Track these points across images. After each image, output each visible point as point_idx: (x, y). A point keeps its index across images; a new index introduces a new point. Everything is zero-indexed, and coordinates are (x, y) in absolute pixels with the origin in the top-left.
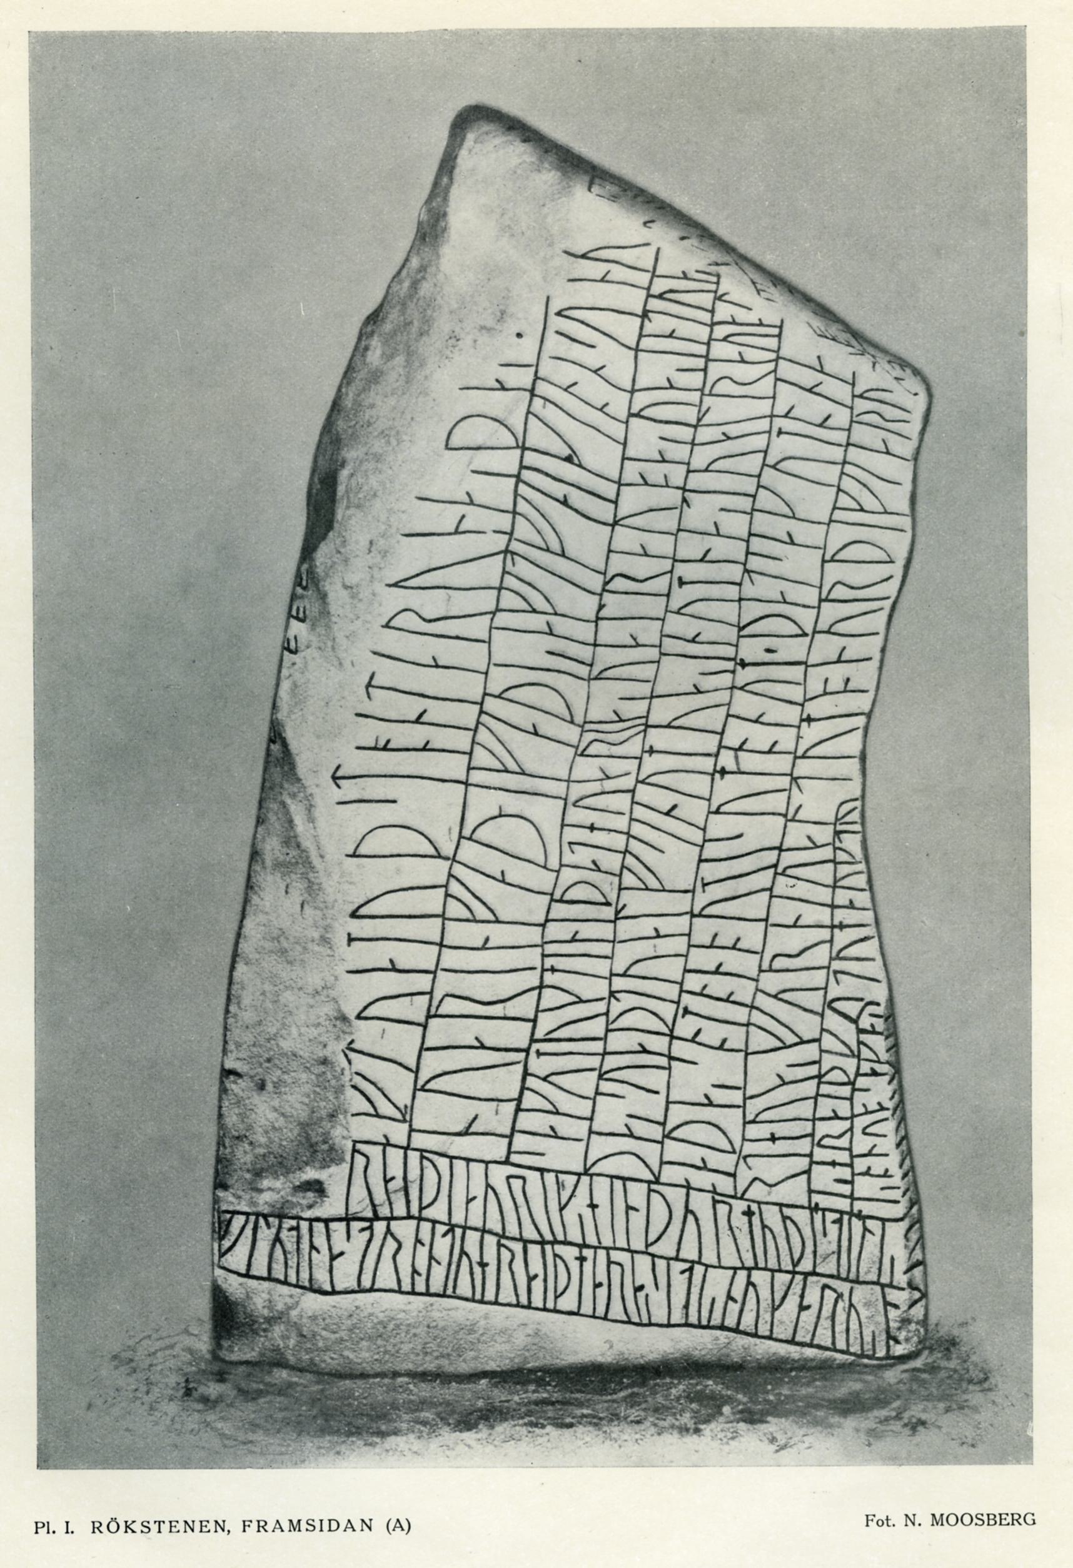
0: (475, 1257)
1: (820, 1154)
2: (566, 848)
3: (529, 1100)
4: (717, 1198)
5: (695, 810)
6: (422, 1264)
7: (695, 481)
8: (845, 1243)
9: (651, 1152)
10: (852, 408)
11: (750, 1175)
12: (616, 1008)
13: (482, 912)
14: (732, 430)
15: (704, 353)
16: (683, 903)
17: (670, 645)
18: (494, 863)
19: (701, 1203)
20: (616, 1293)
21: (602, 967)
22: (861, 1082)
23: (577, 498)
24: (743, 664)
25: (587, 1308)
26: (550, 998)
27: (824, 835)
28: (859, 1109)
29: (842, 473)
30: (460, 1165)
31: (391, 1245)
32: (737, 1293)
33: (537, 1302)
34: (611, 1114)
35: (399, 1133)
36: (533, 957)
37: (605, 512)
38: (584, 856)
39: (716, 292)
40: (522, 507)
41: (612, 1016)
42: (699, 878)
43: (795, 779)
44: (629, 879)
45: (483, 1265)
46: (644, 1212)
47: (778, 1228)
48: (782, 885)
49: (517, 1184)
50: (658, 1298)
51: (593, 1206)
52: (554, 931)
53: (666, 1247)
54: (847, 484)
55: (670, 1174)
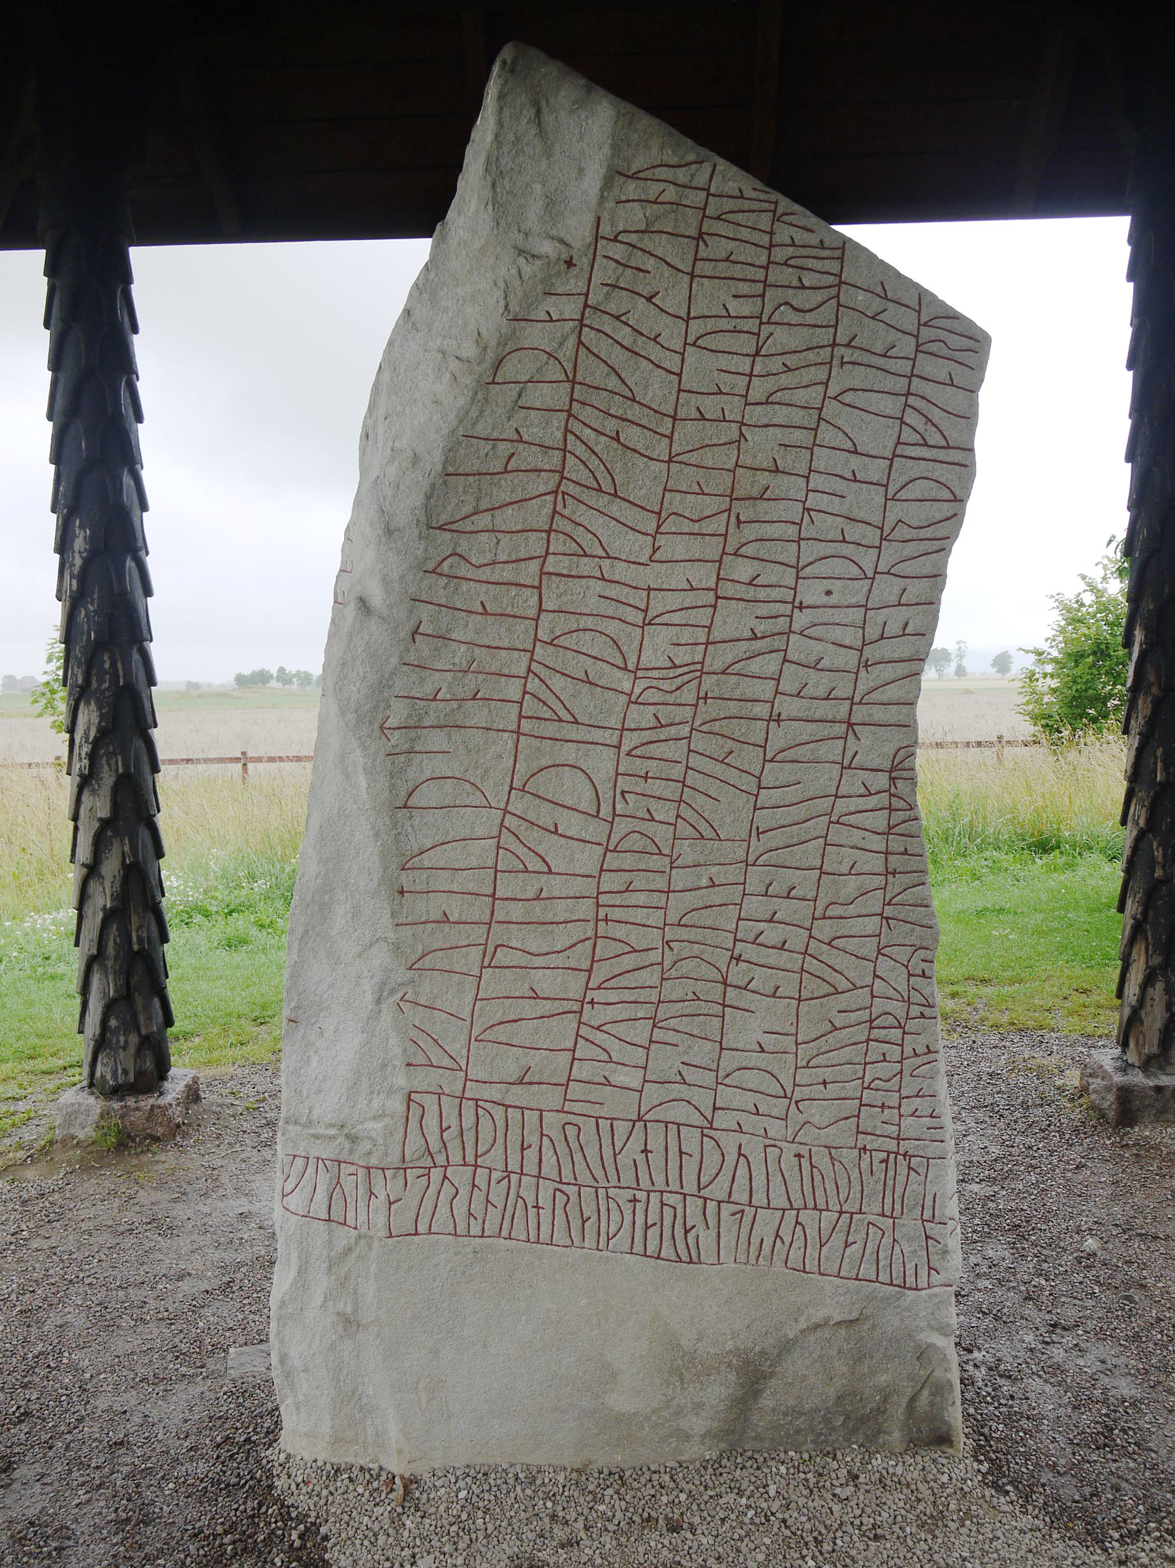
0: (530, 1202)
2: (618, 797)
3: (583, 1050)
5: (750, 758)
6: (477, 1207)
8: (890, 1183)
10: (917, 337)
11: (802, 1118)
13: (535, 864)
14: (791, 360)
15: (763, 278)
17: (727, 589)
19: (754, 1150)
20: (667, 1233)
21: (656, 918)
23: (631, 435)
24: (801, 608)
25: (638, 1247)
27: (882, 781)
28: (908, 1051)
29: (906, 405)
31: (447, 1189)
32: (785, 1233)
34: (664, 1062)
36: (585, 908)
37: (661, 449)
39: (774, 212)
41: (667, 965)
42: (754, 827)
43: (850, 725)
44: (684, 829)
45: (537, 1207)
49: (571, 1131)
50: (707, 1238)
52: (609, 882)
53: (718, 1190)
54: (911, 418)
55: (721, 1120)
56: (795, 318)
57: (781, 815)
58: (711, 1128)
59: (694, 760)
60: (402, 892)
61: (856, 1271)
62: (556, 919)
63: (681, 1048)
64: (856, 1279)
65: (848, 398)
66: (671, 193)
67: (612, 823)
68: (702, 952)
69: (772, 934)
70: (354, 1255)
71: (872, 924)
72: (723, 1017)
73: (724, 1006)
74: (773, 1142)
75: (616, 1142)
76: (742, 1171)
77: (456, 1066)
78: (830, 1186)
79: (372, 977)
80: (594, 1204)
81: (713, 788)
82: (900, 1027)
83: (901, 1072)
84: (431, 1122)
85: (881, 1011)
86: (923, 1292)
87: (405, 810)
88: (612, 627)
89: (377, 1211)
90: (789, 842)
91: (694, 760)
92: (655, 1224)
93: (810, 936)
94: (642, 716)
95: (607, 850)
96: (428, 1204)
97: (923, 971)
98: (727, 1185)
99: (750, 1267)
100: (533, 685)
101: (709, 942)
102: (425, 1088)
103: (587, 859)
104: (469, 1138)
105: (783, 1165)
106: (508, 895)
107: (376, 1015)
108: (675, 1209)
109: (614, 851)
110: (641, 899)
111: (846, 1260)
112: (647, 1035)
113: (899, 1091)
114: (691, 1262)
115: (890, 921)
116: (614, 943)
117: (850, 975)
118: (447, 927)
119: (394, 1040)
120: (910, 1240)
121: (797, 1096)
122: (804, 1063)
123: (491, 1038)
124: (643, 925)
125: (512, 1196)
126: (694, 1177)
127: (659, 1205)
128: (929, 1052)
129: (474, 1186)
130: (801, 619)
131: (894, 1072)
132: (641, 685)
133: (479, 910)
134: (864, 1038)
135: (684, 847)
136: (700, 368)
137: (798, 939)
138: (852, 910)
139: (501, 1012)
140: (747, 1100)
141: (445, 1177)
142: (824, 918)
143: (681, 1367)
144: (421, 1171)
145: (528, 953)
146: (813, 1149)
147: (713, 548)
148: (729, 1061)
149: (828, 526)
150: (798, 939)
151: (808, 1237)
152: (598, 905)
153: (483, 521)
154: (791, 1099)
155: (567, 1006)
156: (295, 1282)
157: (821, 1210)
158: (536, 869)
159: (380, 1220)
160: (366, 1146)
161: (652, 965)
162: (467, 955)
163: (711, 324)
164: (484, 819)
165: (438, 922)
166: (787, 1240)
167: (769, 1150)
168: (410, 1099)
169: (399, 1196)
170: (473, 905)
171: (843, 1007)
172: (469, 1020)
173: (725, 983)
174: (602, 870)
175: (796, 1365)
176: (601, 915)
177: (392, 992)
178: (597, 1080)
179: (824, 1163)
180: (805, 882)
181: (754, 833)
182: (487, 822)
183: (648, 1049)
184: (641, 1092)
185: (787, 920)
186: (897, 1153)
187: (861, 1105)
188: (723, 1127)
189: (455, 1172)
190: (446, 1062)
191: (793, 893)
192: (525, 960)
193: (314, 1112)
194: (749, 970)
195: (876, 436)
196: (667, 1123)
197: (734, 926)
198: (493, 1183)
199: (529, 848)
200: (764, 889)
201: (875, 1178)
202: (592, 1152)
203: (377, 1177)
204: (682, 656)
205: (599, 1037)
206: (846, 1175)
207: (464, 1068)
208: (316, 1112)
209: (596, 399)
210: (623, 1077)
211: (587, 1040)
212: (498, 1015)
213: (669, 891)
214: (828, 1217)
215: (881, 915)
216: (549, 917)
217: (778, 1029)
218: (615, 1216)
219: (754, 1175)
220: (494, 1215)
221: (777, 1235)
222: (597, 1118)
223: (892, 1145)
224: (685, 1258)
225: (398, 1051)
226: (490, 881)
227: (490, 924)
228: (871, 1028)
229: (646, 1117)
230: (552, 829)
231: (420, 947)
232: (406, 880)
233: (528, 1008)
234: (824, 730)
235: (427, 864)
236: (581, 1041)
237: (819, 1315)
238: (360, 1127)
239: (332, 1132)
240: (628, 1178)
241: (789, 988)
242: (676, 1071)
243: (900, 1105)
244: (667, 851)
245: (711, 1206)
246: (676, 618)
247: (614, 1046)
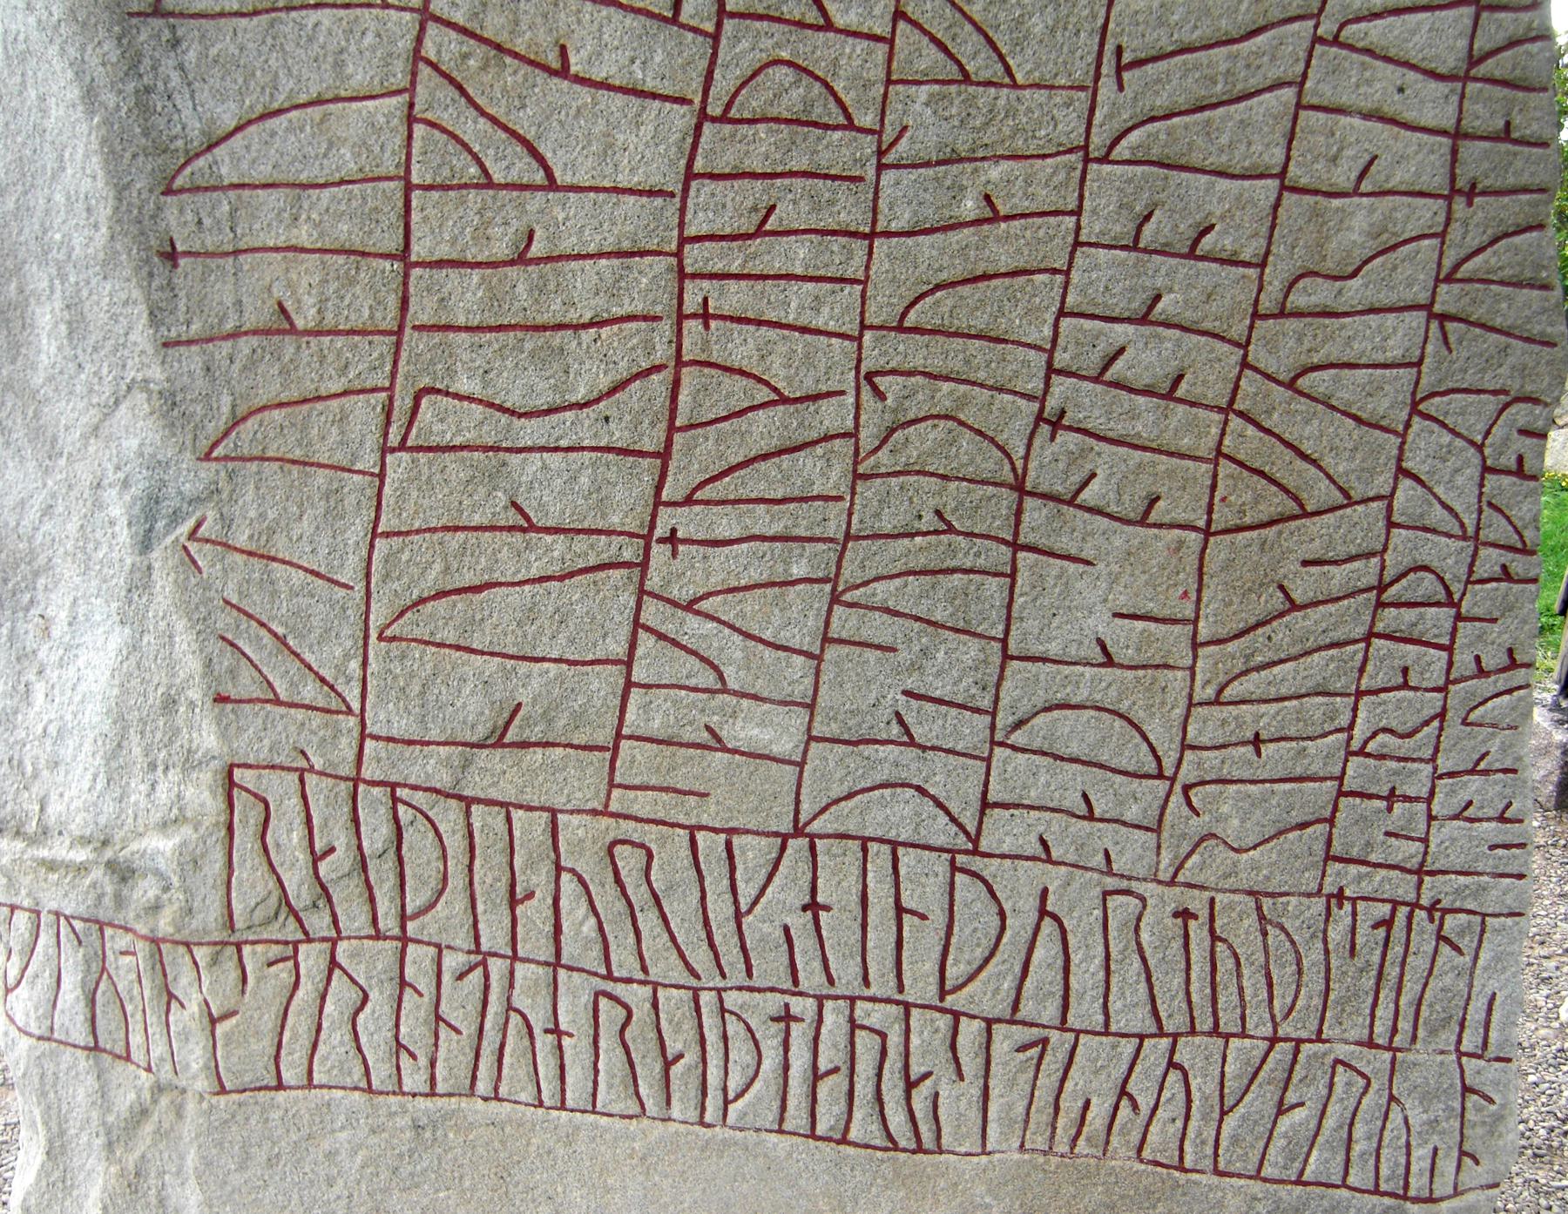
0: (539, 1021)
3: (651, 661)
4: (1117, 885)
6: (414, 1028)
8: (1392, 972)
11: (1196, 825)
13: (510, 165)
20: (864, 1089)
21: (837, 309)
22: (1476, 600)
28: (1464, 660)
34: (860, 689)
36: (647, 284)
41: (867, 438)
45: (556, 1031)
46: (938, 918)
49: (629, 860)
50: (957, 1101)
51: (813, 907)
53: (987, 995)
55: (1002, 832)
58: (975, 852)
60: (171, 256)
61: (1297, 1165)
62: (572, 316)
63: (903, 656)
64: (1299, 1182)
67: (716, 37)
68: (962, 402)
69: (1147, 357)
70: (148, 1128)
72: (1013, 575)
73: (1016, 546)
74: (1124, 884)
75: (740, 885)
76: (1046, 951)
77: (335, 704)
78: (1252, 981)
79: (126, 484)
80: (689, 1026)
82: (1450, 603)
83: (1442, 715)
84: (288, 837)
85: (1407, 562)
86: (1444, 1205)
87: (157, 23)
89: (186, 1036)
90: (1202, 93)
92: (836, 1070)
93: (1245, 364)
95: (703, 116)
96: (298, 1023)
97: (1520, 459)
98: (1008, 985)
99: (1054, 1160)
101: (981, 376)
102: (264, 756)
103: (647, 145)
105: (1145, 936)
106: (444, 252)
107: (141, 581)
108: (883, 1036)
109: (724, 119)
110: (799, 254)
111: (1278, 1143)
112: (814, 623)
113: (1433, 759)
114: (919, 1149)
115: (1450, 326)
116: (728, 380)
117: (1339, 468)
118: (289, 345)
119: (184, 641)
120: (1426, 1098)
121: (1187, 774)
122: (1210, 692)
123: (417, 633)
124: (804, 330)
126: (931, 966)
127: (846, 1027)
128: (1513, 664)
129: (403, 983)
131: (1428, 712)
133: (368, 297)
134: (1360, 631)
135: (916, 105)
137: (1210, 371)
138: (1355, 292)
139: (438, 567)
140: (1068, 784)
141: (333, 964)
142: (1282, 314)
144: (276, 951)
145: (501, 409)
146: (1219, 897)
150: (1210, 371)
151: (1196, 1095)
152: (682, 275)
154: (1173, 780)
155: (606, 549)
156: (44, 1172)
157: (1227, 1037)
158: (513, 177)
159: (195, 1056)
160: (145, 890)
161: (827, 438)
162: (343, 418)
164: (369, 39)
165: (267, 332)
166: (1145, 1103)
167: (1113, 901)
168: (230, 784)
169: (230, 1005)
170: (352, 282)
171: (1314, 550)
172: (360, 587)
173: (1019, 487)
174: (690, 176)
176: (692, 303)
177: (176, 518)
178: (688, 735)
179: (1241, 928)
181: (1107, 68)
183: (819, 658)
184: (801, 765)
185: (1188, 316)
186: (1415, 905)
187: (1341, 793)
188: (1005, 849)
189: (353, 955)
190: (310, 691)
191: (1207, 242)
192: (493, 429)
193: (50, 810)
194: (1084, 452)
196: (865, 842)
197: (1047, 331)
198: (447, 978)
199: (494, 120)
200: (1131, 227)
201: (1359, 962)
202: (682, 909)
203: (177, 960)
205: (693, 628)
206: (1291, 957)
207: (356, 706)
208: (55, 809)
210: (747, 730)
211: (661, 636)
212: (432, 575)
213: (871, 236)
215: (1428, 307)
216: (554, 310)
217: (1151, 607)
218: (741, 1052)
219: (1075, 958)
220: (453, 1051)
221: (1123, 1092)
222: (693, 830)
223: (1403, 887)
224: (905, 1139)
225: (192, 665)
226: (392, 216)
227: (399, 332)
228: (1380, 605)
229: (815, 827)
230: (553, 61)
231: (226, 400)
232: (177, 219)
233: (505, 556)
235: (228, 174)
236: (646, 642)
238: (134, 846)
239: (81, 855)
240: (770, 967)
241: (1182, 505)
242: (888, 713)
243: (1432, 793)
244: (867, 119)
245: (970, 1031)
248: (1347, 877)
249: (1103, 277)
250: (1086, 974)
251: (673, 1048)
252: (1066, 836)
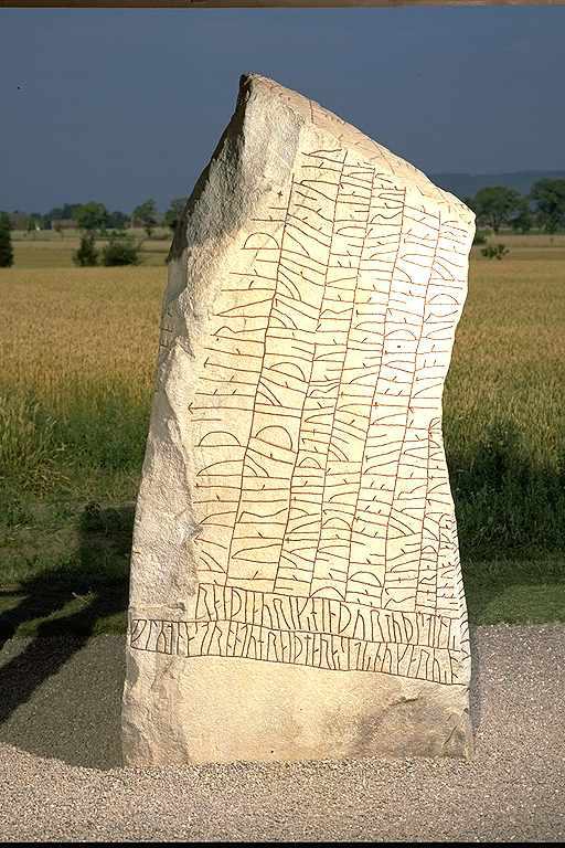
0: (257, 638)
1: (421, 587)
3: (284, 562)
4: (374, 610)
5: (363, 424)
6: (232, 642)
7: (364, 265)
8: (432, 630)
9: (341, 587)
11: (388, 598)
12: (325, 518)
13: (260, 472)
14: (381, 240)
16: (357, 467)
17: (351, 344)
18: (267, 450)
19: (365, 612)
22: (441, 552)
23: (307, 273)
25: (310, 662)
26: (295, 514)
27: (424, 434)
28: (440, 566)
30: (250, 595)
32: (381, 654)
33: (272, 657)
35: (221, 579)
37: (320, 280)
38: (309, 445)
40: (281, 277)
47: (401, 623)
48: (405, 460)
49: (278, 603)
50: (343, 657)
52: (297, 481)
54: (436, 266)
55: (350, 597)
56: (382, 221)
57: (379, 451)
59: (337, 424)
65: (408, 258)
66: (327, 164)
71: (421, 503)
78: (403, 630)
81: (349, 439)
88: (302, 363)
91: (337, 424)
94: (311, 403)
96: (208, 639)
100: (261, 388)
103: (286, 471)
104: (228, 606)
121: (386, 587)
125: (248, 637)
130: (386, 359)
132: (311, 389)
133: (235, 495)
136: (340, 244)
137: (386, 509)
140: (360, 588)
143: (332, 723)
147: (345, 326)
148: (354, 569)
149: (397, 317)
150: (386, 509)
153: (235, 312)
163: (346, 224)
166: (382, 658)
175: (388, 724)
179: (398, 617)
180: (390, 483)
182: (239, 453)
190: (218, 568)
195: (420, 276)
204: (331, 376)
209: (290, 256)
214: (402, 647)
218: (299, 647)
223: (432, 611)
234: (395, 410)
237: (398, 696)
246: (330, 358)
247: (297, 560)
248: (423, 610)
249: (366, 494)
250: (368, 629)
251: (285, 645)
252: (365, 600)
